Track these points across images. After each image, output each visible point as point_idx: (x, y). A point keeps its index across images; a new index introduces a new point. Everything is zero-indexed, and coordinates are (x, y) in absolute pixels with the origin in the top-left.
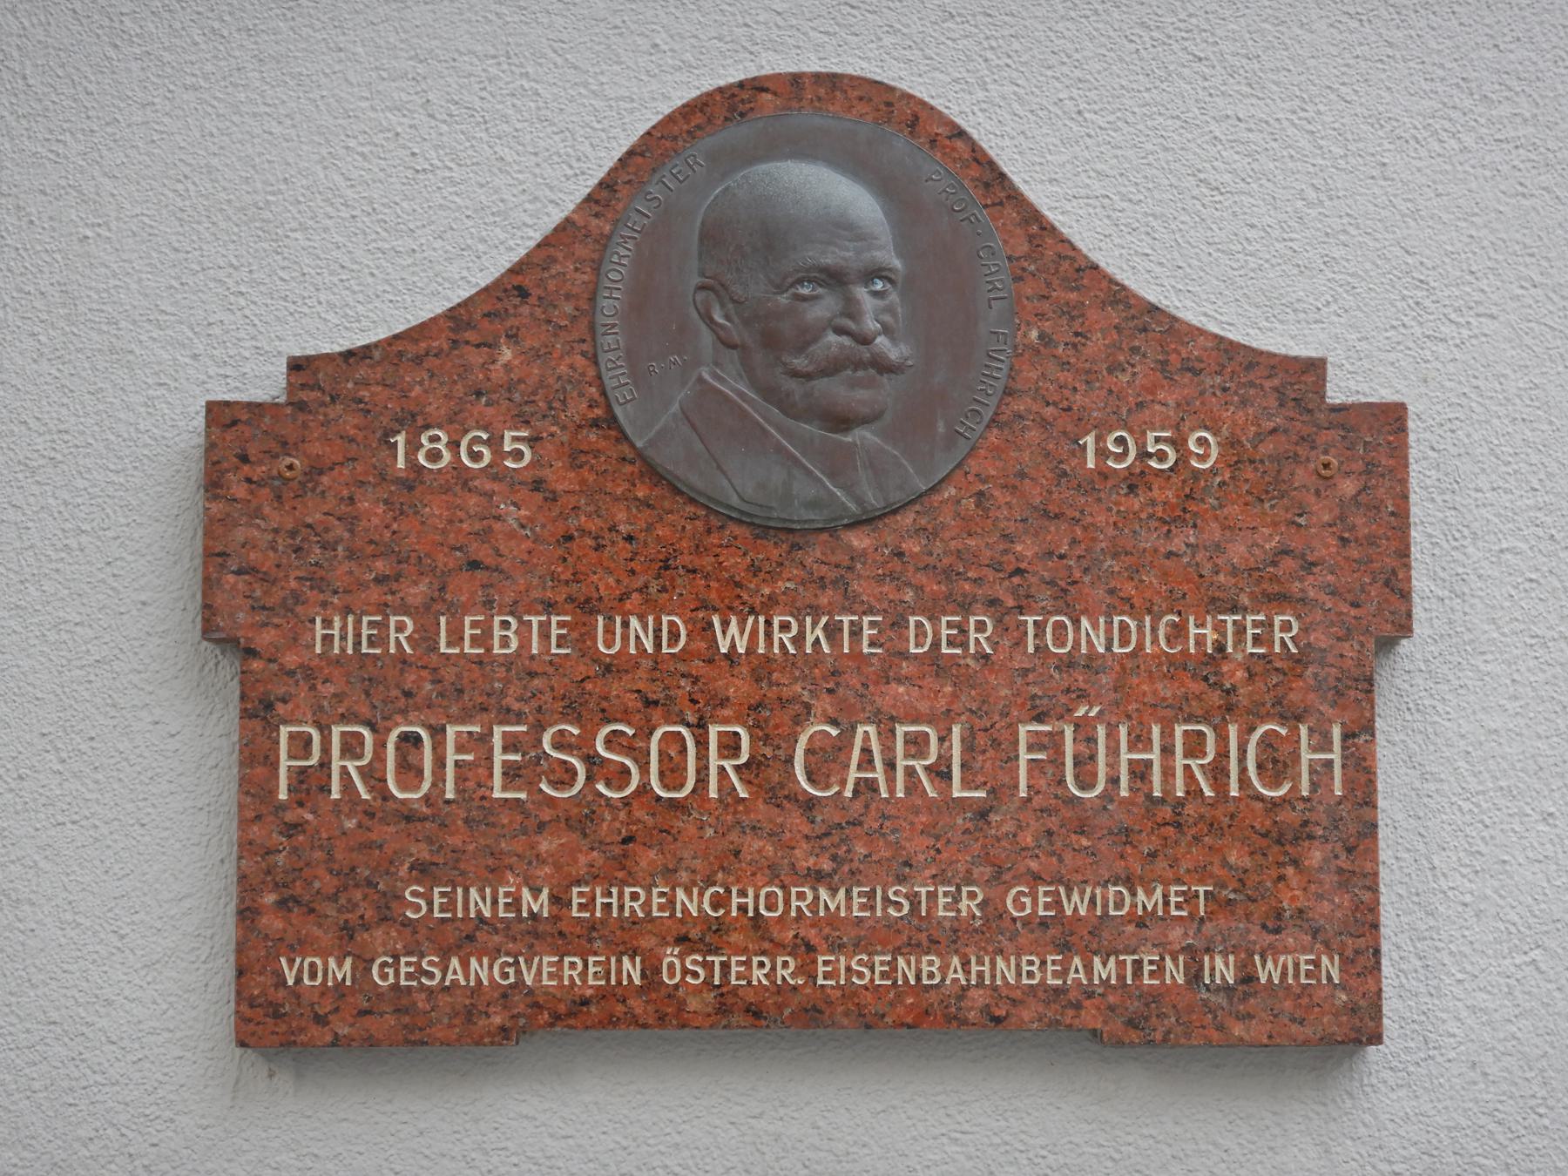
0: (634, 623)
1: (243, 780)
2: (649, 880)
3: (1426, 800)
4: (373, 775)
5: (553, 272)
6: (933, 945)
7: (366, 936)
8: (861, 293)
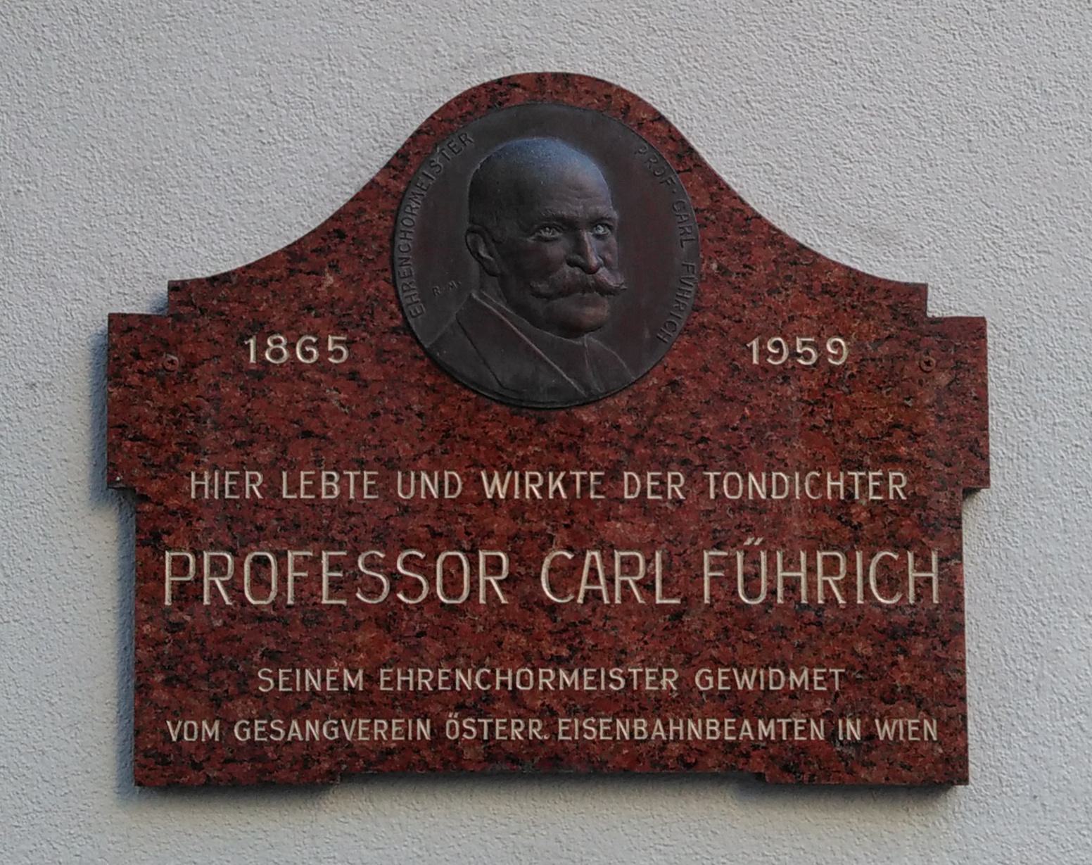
0: (424, 476)
1: (139, 591)
2: (436, 663)
3: (1000, 605)
4: (234, 587)
6: (642, 711)
7: (229, 705)
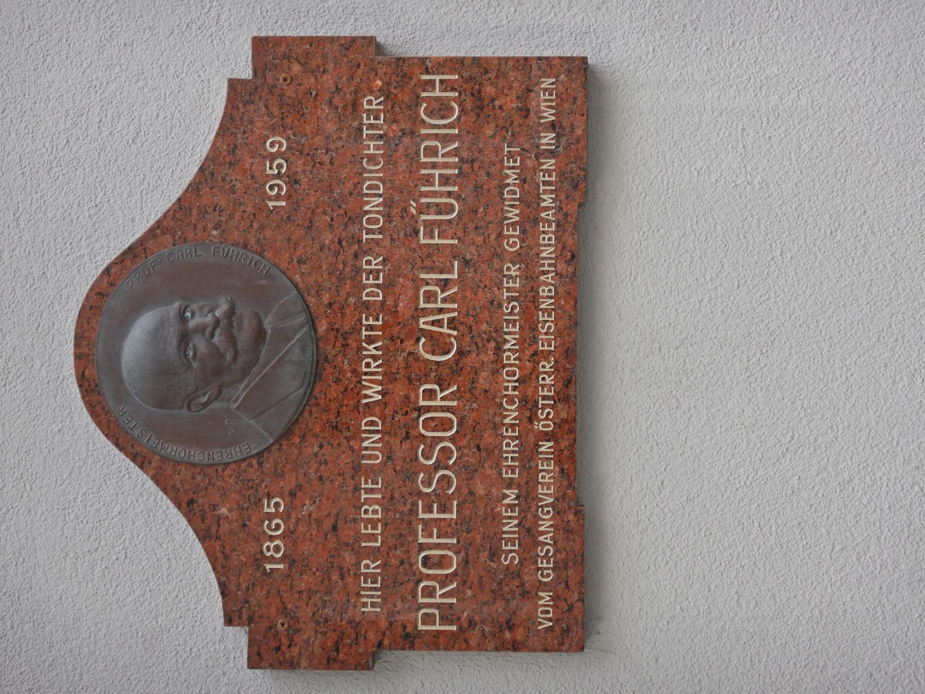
0: (365, 444)
1: (446, 649)
2: (500, 437)
3: (461, 30)
4: (444, 581)
5: (180, 486)
6: (534, 290)
7: (527, 585)
8: (192, 324)
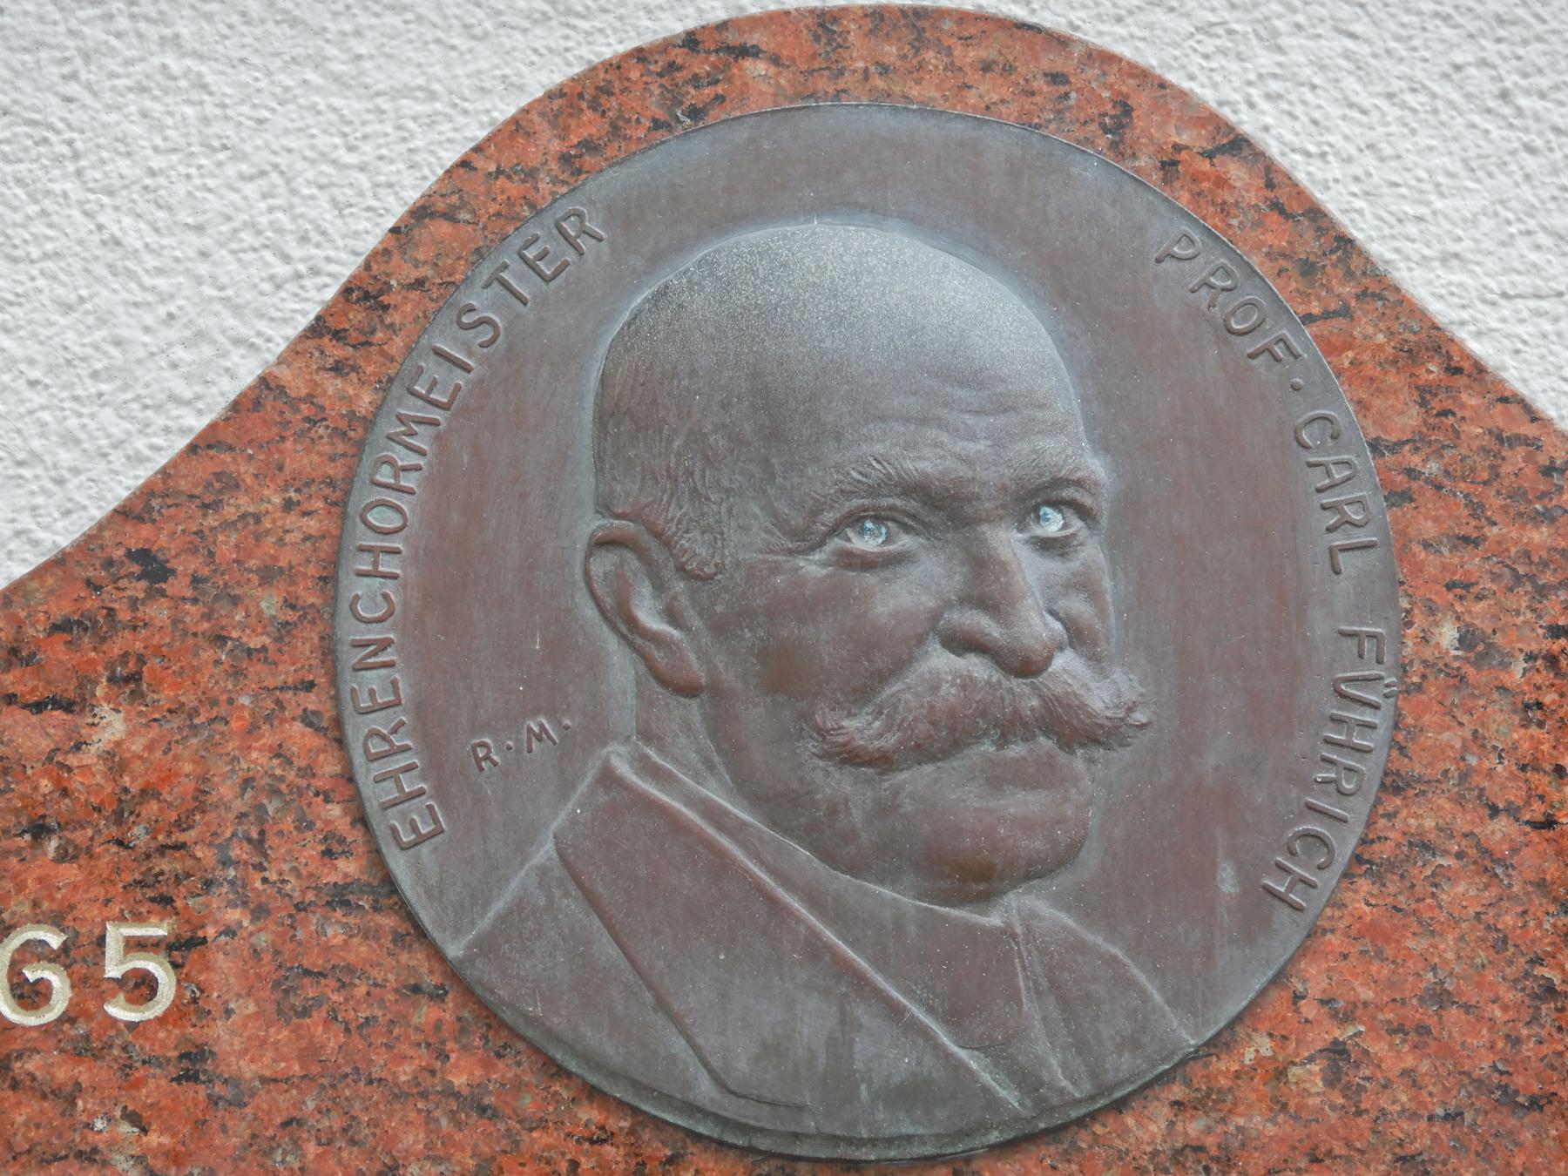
5: (230, 512)
8: (1007, 542)
